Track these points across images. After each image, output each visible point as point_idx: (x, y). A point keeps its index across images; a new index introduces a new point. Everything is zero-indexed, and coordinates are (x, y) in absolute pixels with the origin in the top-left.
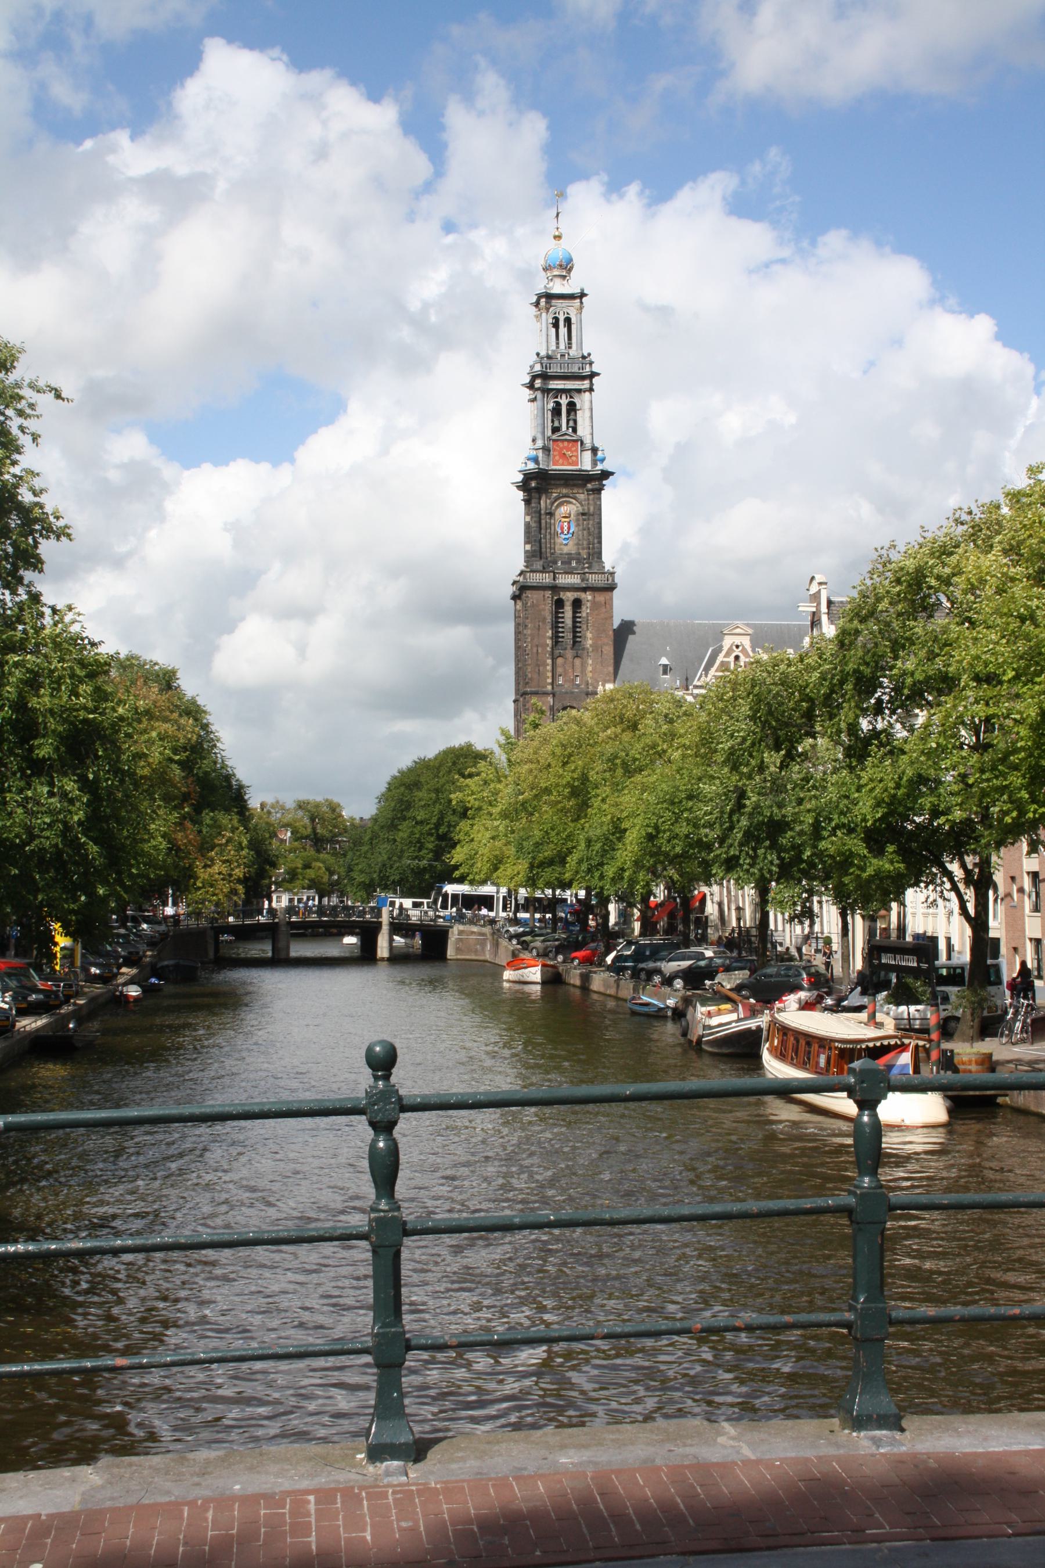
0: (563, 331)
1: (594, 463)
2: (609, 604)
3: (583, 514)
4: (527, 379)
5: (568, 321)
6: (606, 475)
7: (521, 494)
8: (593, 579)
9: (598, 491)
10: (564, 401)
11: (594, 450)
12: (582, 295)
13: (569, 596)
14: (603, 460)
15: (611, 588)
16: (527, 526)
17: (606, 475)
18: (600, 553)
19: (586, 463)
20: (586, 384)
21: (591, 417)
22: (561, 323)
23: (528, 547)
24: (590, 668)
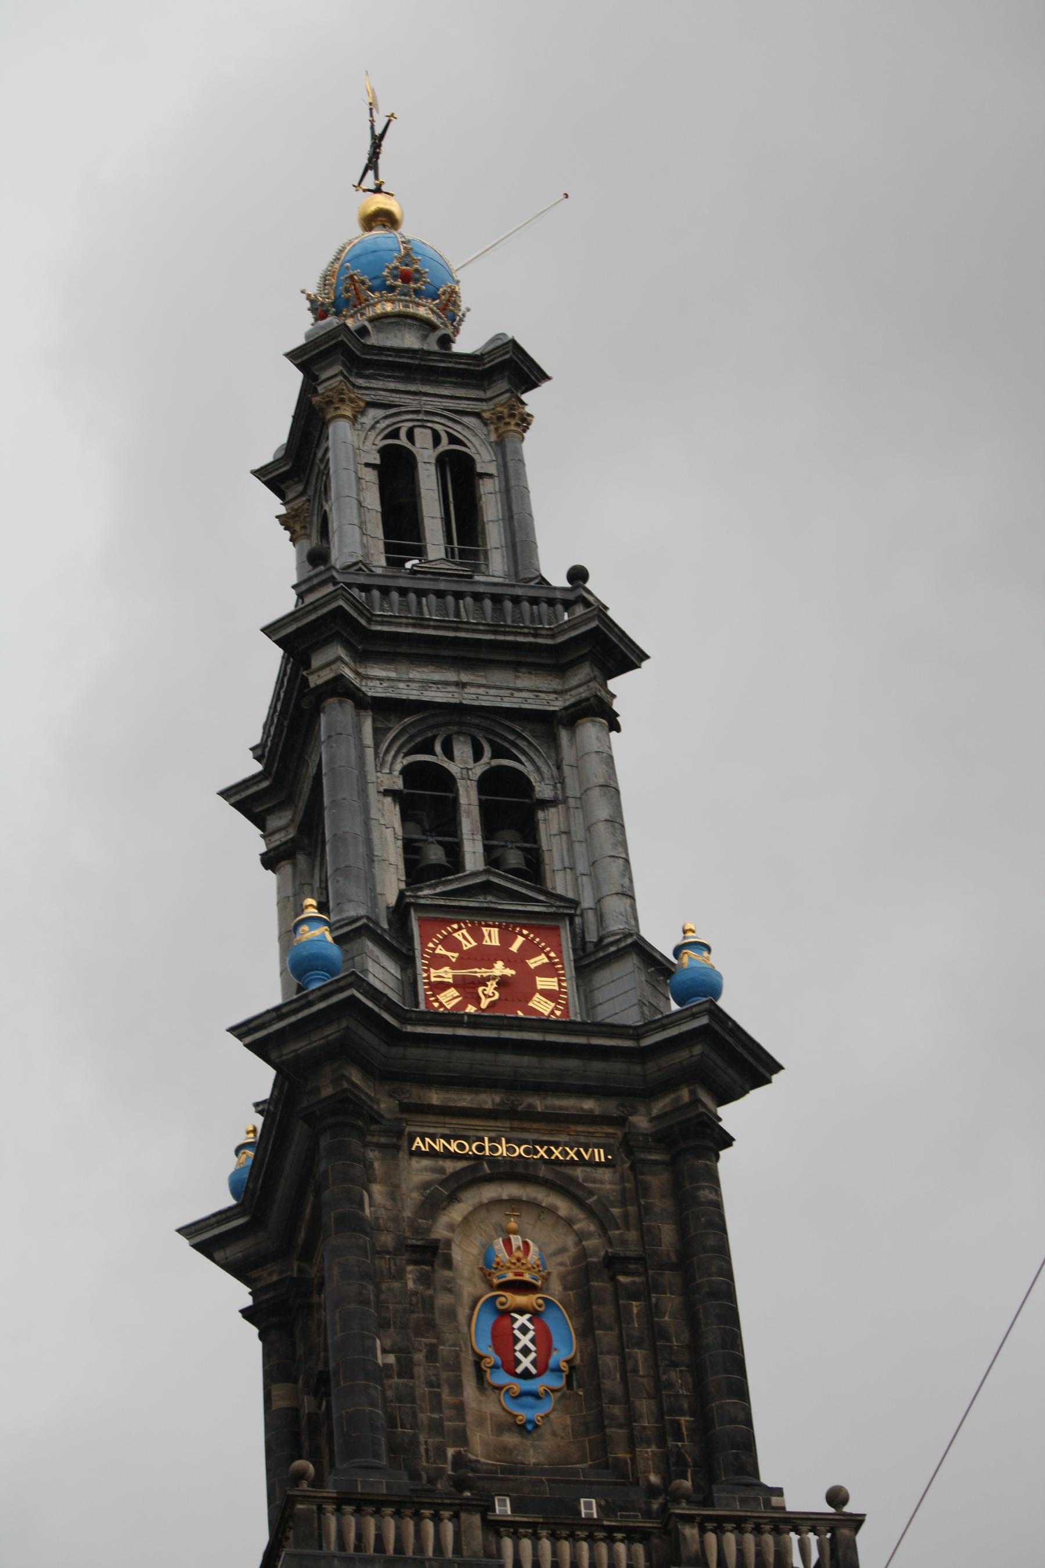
3: (613, 1264)
5: (459, 472)
10: (465, 767)
18: (747, 1445)
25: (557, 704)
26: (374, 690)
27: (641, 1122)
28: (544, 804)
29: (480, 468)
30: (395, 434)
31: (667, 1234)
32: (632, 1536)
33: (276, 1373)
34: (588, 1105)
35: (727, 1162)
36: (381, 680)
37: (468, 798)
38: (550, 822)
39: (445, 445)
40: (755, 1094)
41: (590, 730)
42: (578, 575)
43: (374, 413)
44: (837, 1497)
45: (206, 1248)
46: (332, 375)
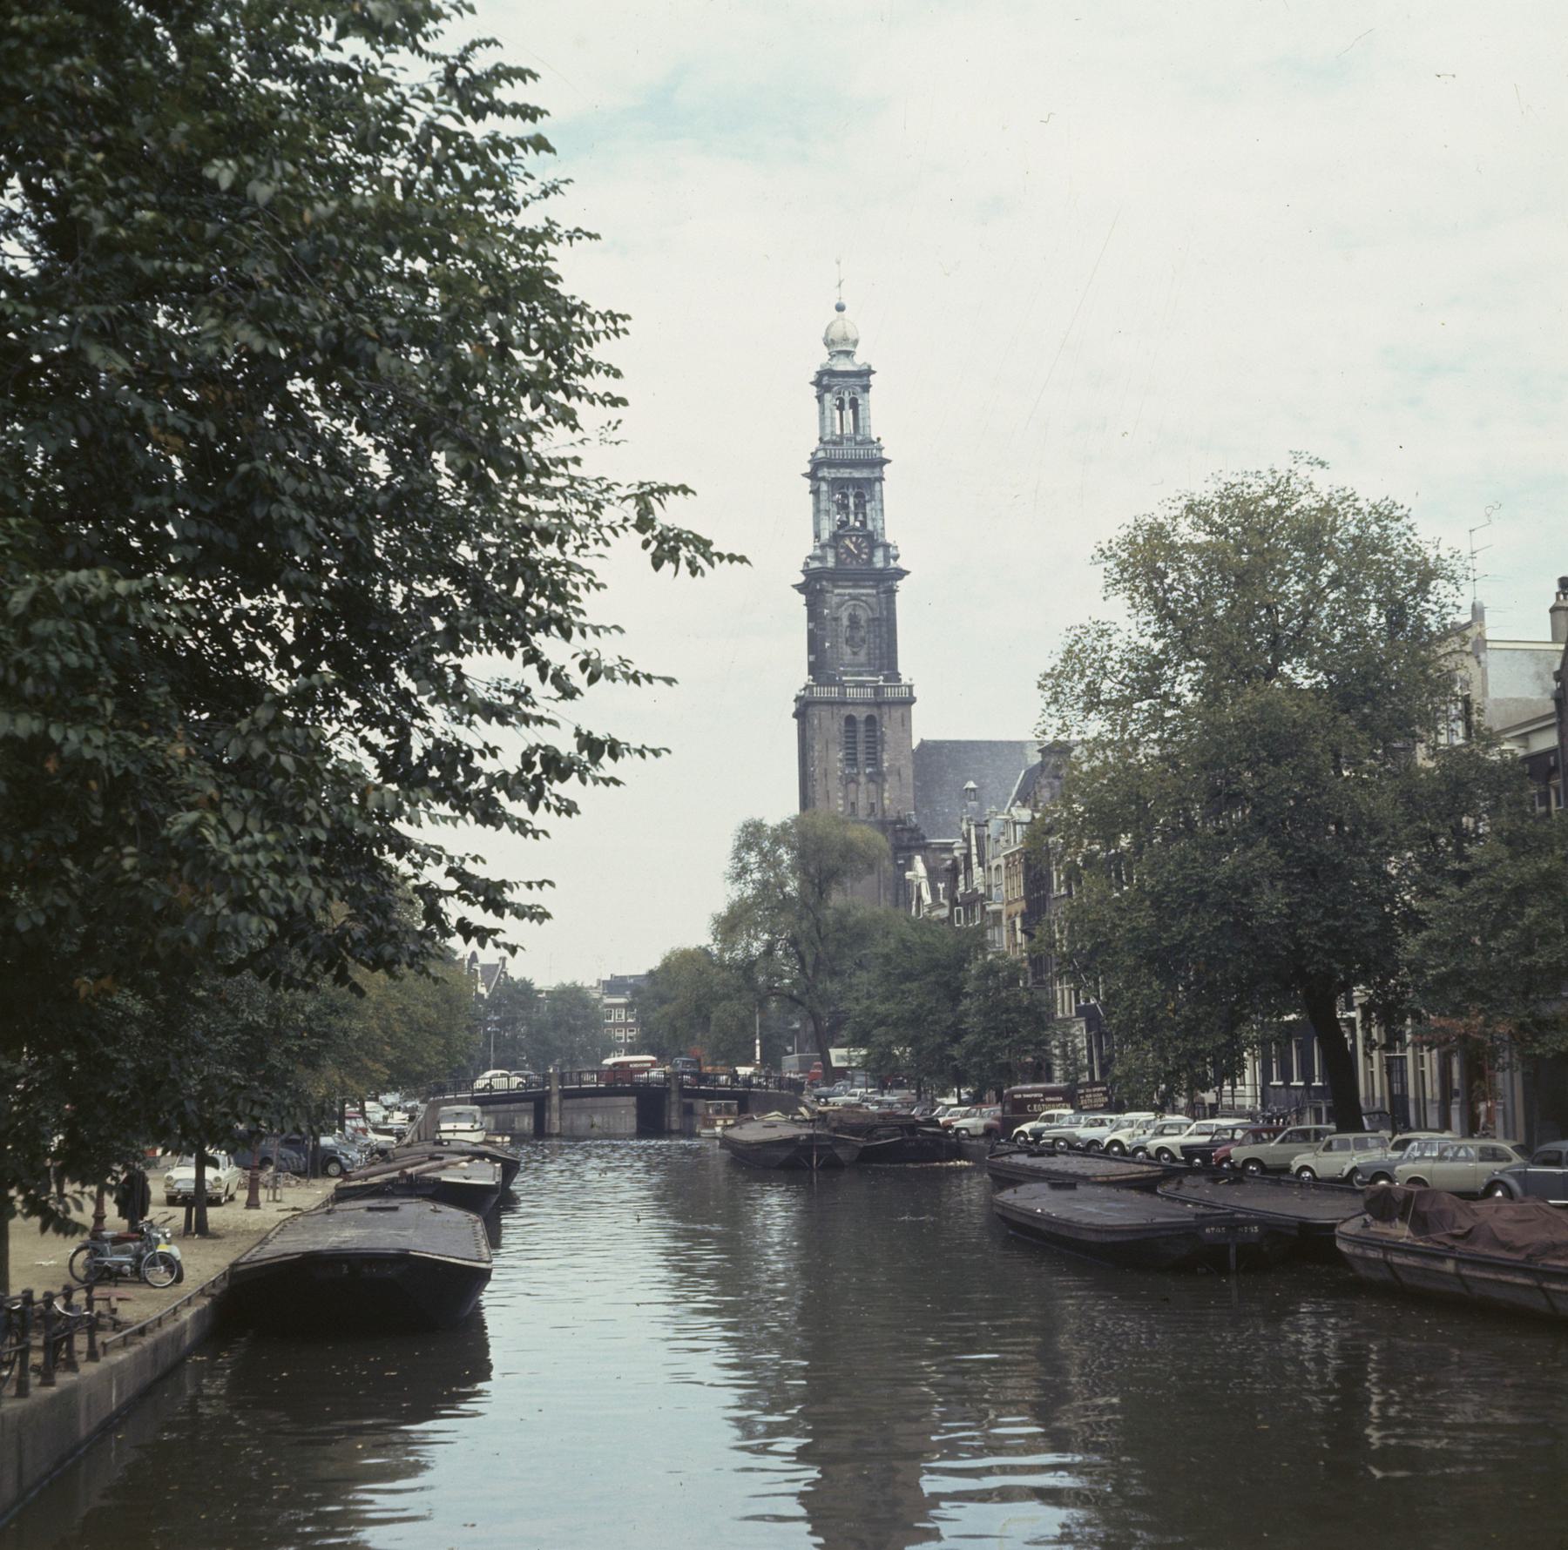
0: (848, 414)
1: (887, 558)
2: (906, 722)
3: (874, 620)
4: (808, 469)
6: (901, 574)
7: (802, 598)
8: (889, 693)
9: (892, 592)
11: (886, 546)
12: (870, 372)
13: (861, 713)
14: (896, 558)
15: (911, 701)
16: (811, 633)
17: (901, 574)
19: (879, 562)
22: (847, 406)
23: (812, 658)
24: (886, 795)
37: (851, 500)
38: (868, 507)
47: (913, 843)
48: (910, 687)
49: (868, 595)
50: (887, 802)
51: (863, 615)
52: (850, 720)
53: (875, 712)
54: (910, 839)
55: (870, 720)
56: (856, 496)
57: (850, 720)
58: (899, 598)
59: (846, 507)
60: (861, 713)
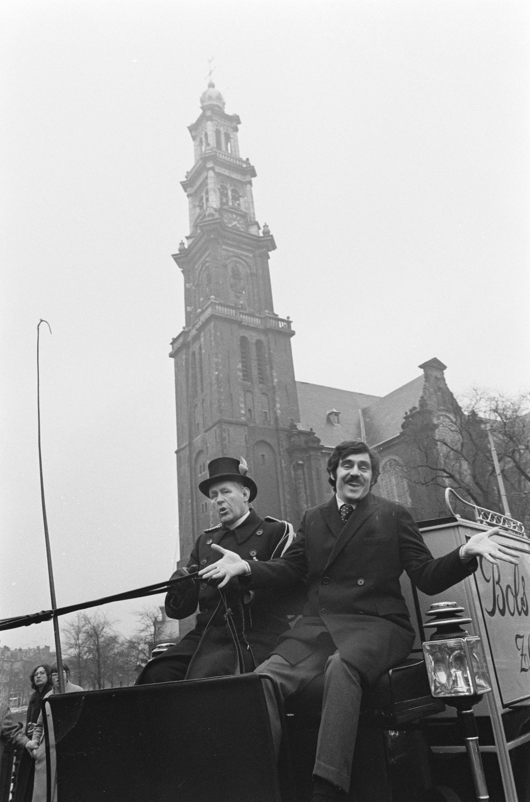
3: (252, 274)
13: (253, 337)
20: (247, 178)
21: (253, 202)
24: (278, 405)
25: (244, 181)
26: (217, 170)
27: (257, 252)
28: (241, 197)
29: (232, 136)
30: (217, 126)
31: (260, 272)
32: (258, 318)
33: (186, 281)
34: (249, 248)
35: (269, 261)
36: (217, 169)
37: (230, 193)
39: (225, 131)
40: (273, 251)
41: (248, 186)
42: (248, 159)
43: (214, 122)
44: (288, 318)
45: (175, 259)
46: (209, 113)
47: (311, 444)
48: (289, 323)
49: (247, 256)
50: (279, 411)
51: (243, 271)
52: (244, 340)
53: (263, 338)
54: (306, 442)
55: (259, 343)
56: (233, 191)
57: (244, 340)
58: (271, 262)
59: (226, 195)
60: (253, 337)
